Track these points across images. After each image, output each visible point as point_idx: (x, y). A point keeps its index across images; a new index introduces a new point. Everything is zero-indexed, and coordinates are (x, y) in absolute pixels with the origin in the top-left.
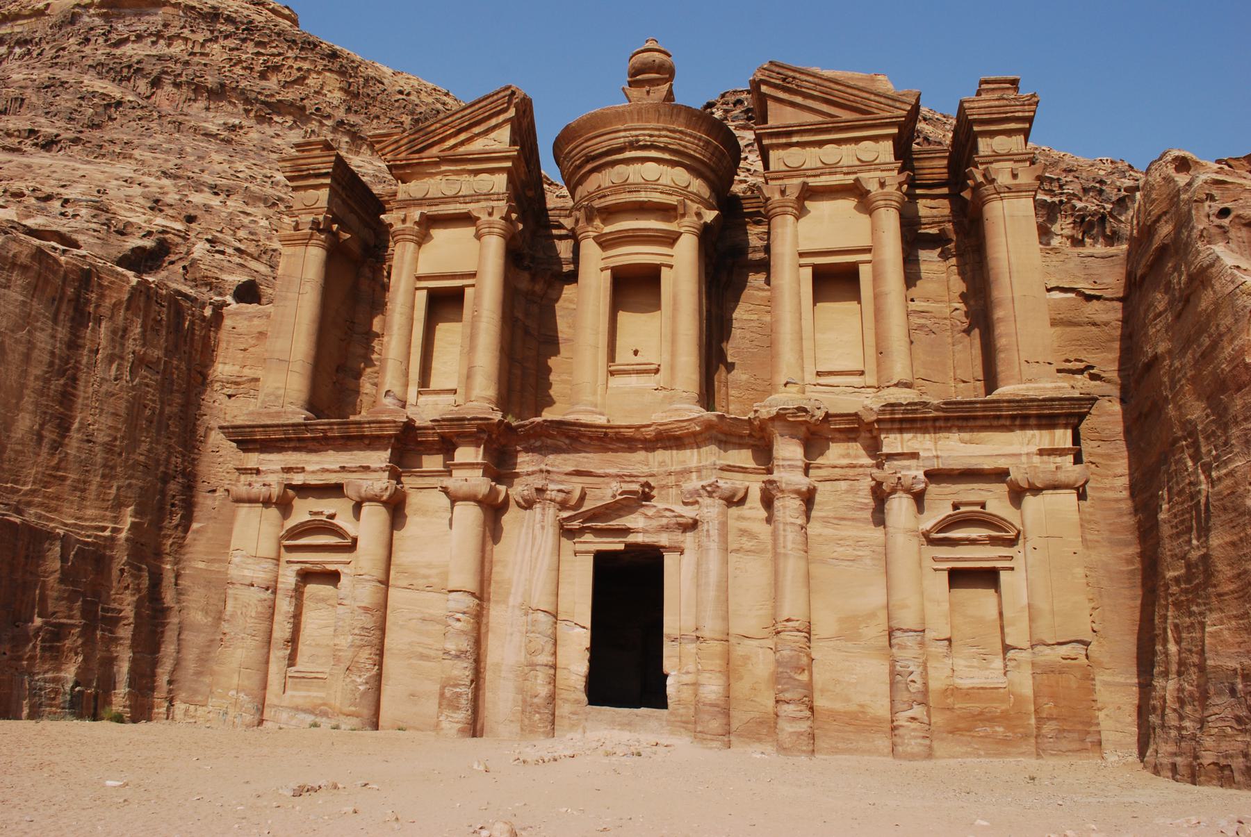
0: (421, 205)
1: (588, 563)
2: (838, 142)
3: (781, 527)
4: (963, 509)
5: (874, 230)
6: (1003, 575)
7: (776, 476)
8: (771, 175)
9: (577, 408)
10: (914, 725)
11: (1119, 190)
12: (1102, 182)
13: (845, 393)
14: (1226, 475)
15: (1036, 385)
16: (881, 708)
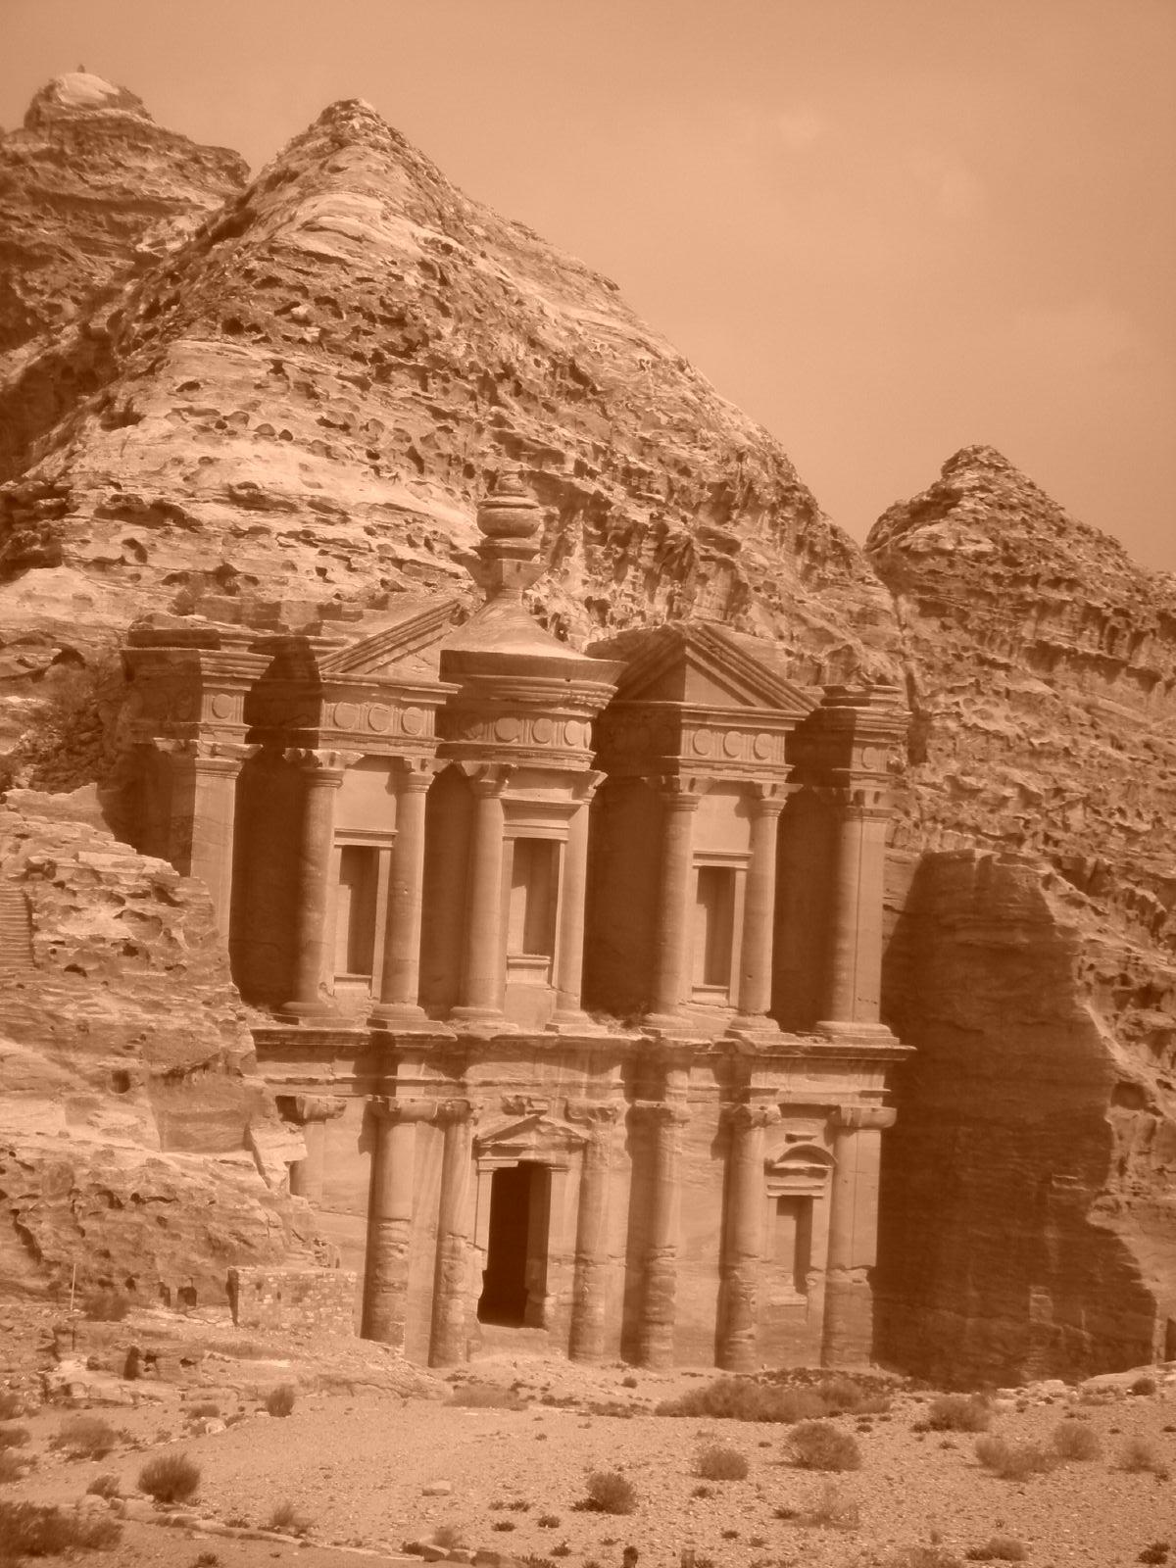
0: (349, 740)
1: (487, 1183)
2: (742, 730)
3: (668, 1155)
4: (799, 1143)
5: (754, 839)
6: (816, 1204)
7: (669, 1103)
8: (685, 763)
9: (481, 1009)
10: (749, 1341)
11: (702, 487)
12: (685, 472)
13: (713, 1012)
14: (1069, 1192)
15: (865, 1026)
16: (710, 1322)
